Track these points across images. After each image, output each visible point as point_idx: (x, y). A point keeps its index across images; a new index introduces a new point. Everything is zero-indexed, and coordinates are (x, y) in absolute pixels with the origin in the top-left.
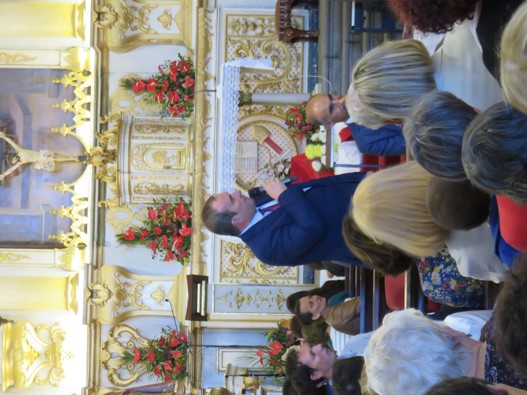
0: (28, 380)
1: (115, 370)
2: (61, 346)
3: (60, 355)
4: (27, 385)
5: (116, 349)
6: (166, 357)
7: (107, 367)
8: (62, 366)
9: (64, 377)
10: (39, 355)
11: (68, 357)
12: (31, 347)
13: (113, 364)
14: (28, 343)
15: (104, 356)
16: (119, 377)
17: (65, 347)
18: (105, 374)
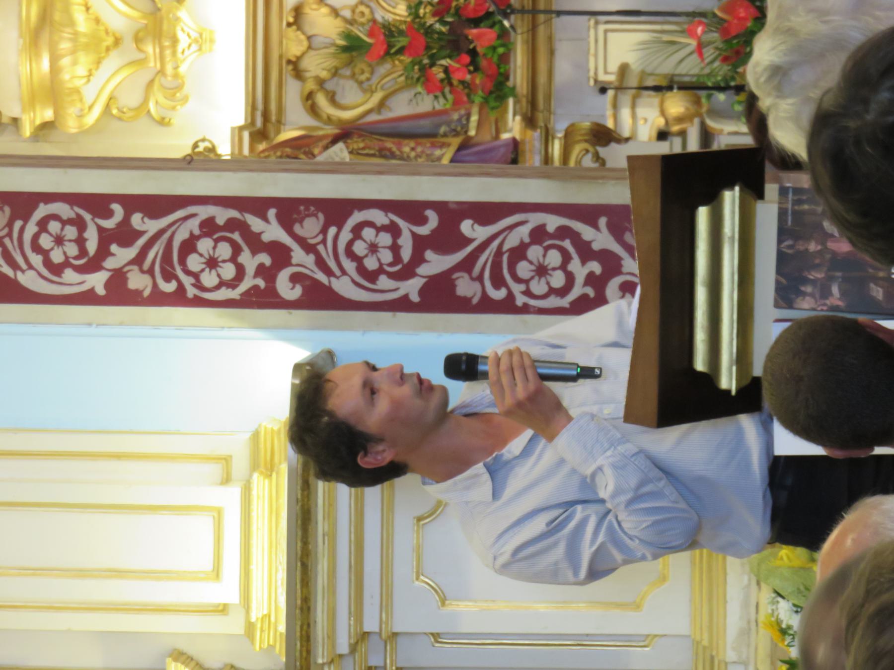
0: (90, 108)
1: (321, 82)
2: (177, 19)
3: (175, 41)
4: (90, 119)
5: (324, 25)
6: (455, 44)
7: (298, 74)
8: (182, 70)
9: (185, 99)
10: (117, 42)
11: (194, 47)
12: (98, 21)
13: (316, 65)
14: (88, 9)
15: (294, 45)
16: (332, 99)
17: (186, 22)
18: (293, 91)
